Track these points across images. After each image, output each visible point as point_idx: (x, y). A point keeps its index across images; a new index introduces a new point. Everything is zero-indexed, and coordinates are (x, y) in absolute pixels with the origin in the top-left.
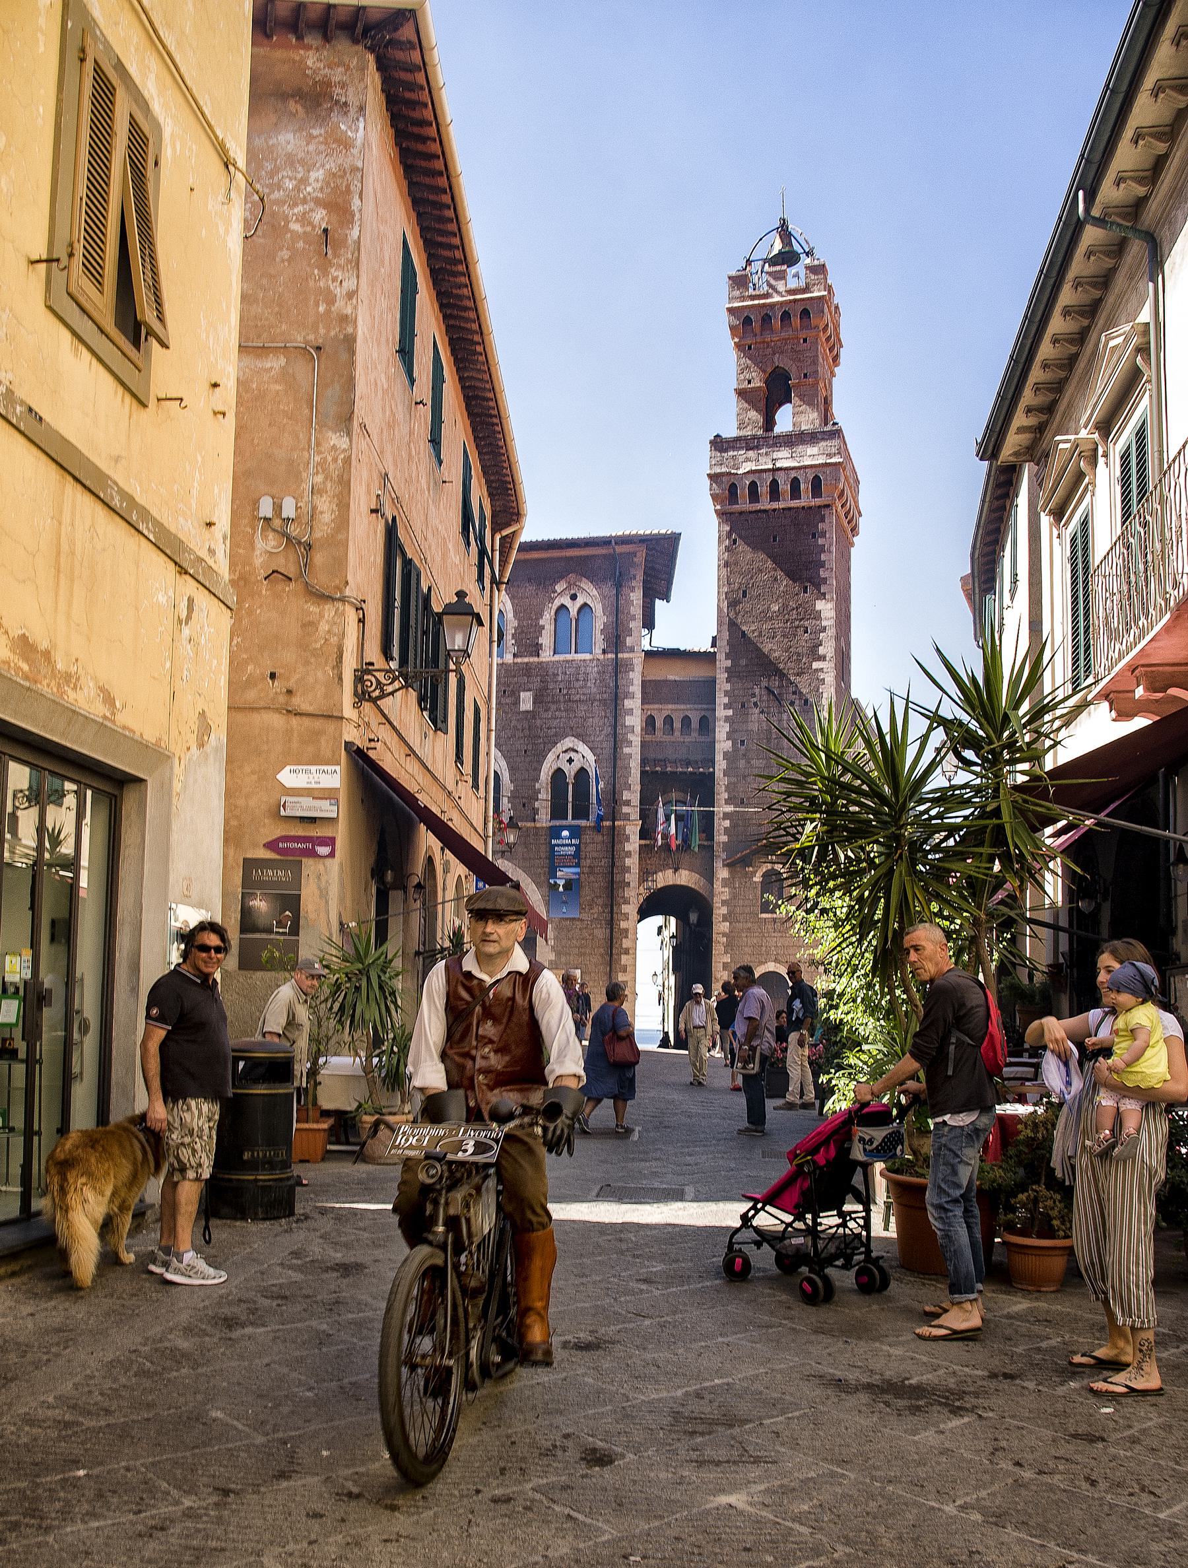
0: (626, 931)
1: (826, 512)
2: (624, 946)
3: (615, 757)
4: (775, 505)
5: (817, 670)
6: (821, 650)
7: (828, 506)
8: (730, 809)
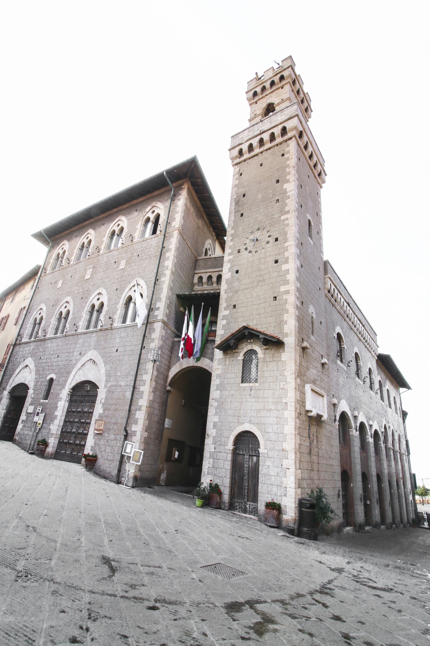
0: (142, 393)
1: (288, 142)
2: (139, 404)
3: (155, 283)
4: (262, 149)
5: (284, 220)
6: (287, 209)
7: (290, 139)
8: (227, 313)
